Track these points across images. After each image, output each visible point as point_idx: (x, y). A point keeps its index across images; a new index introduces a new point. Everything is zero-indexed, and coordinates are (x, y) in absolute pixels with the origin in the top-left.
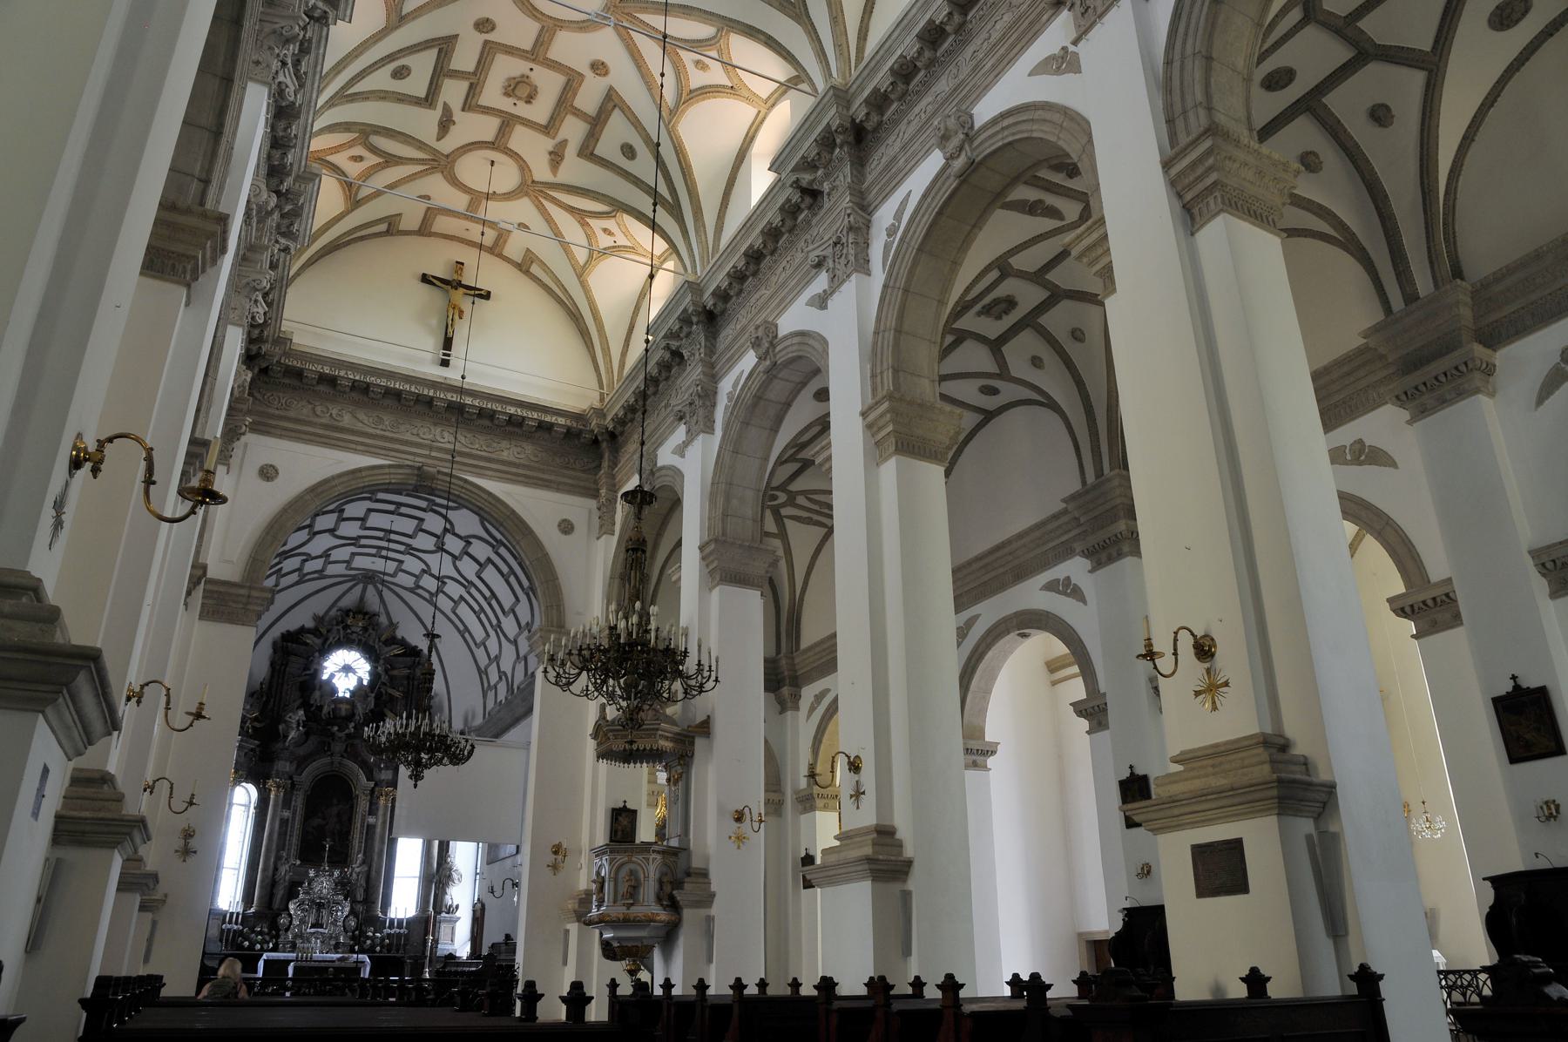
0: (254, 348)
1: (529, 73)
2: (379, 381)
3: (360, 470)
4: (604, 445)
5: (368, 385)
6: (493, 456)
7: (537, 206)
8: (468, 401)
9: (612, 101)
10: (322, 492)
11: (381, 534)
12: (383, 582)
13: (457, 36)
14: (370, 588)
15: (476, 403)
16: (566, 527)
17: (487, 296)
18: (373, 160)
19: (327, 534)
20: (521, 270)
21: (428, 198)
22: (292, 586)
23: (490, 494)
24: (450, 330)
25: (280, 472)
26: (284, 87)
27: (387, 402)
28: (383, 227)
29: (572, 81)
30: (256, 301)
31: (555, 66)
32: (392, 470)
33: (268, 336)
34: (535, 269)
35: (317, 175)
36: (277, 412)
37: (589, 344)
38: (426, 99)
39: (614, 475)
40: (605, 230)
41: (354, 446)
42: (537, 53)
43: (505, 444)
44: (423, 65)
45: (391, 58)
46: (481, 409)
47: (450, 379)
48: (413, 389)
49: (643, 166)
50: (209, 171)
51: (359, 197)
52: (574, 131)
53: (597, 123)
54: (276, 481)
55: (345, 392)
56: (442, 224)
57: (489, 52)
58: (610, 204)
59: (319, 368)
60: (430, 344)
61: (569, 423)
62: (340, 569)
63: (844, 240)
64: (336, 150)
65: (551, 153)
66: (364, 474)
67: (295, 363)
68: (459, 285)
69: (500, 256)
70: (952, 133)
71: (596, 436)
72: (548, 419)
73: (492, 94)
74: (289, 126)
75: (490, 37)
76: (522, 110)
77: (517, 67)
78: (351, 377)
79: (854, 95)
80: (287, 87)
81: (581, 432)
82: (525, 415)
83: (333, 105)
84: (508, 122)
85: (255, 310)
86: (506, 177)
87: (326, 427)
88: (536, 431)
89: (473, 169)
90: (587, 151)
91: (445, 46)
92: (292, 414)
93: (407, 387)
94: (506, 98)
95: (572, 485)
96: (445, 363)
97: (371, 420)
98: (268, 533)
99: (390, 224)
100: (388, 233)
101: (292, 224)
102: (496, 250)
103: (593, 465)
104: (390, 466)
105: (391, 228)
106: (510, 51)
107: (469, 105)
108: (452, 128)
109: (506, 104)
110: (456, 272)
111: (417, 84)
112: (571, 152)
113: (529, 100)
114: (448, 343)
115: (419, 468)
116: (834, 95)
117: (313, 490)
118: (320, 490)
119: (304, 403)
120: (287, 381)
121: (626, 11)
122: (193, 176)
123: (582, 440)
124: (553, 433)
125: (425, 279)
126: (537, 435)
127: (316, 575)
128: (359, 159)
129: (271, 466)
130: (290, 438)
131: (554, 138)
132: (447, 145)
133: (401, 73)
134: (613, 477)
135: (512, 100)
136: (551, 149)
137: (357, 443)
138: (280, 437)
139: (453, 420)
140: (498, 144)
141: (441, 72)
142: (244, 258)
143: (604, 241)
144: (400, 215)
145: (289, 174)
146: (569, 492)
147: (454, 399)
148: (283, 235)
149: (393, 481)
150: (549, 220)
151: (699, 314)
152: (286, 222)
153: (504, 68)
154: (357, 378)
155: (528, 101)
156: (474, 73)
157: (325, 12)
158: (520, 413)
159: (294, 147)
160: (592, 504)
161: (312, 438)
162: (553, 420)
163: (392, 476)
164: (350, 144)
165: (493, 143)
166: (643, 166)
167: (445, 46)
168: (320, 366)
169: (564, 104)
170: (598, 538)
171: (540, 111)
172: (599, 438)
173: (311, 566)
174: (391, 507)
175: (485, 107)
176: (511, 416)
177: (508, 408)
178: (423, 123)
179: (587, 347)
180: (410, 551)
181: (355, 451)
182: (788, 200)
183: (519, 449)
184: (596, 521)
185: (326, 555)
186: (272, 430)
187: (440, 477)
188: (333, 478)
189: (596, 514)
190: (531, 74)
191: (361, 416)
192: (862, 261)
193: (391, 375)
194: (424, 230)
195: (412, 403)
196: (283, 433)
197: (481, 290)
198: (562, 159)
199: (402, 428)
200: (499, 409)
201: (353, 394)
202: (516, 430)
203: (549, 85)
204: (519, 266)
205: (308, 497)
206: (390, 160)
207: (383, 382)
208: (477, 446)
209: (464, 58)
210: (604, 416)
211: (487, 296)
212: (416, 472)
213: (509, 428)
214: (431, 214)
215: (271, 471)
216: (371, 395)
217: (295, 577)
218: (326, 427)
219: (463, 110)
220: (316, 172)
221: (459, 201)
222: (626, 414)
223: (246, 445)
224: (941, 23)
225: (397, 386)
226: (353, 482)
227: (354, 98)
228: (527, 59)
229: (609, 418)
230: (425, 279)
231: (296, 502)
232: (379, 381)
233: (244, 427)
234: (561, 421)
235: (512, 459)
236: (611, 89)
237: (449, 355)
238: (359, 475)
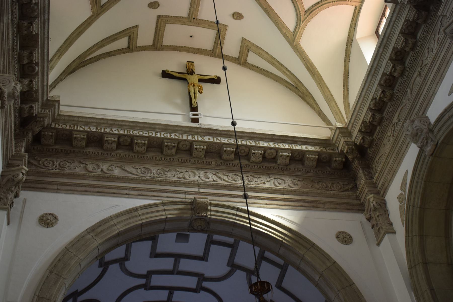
5: (132, 138)
8: (225, 140)
10: (102, 231)
20: (239, 64)
24: (193, 100)
25: (59, 218)
27: (151, 155)
34: (252, 58)
37: (312, 102)
39: (375, 184)
48: (173, 136)
51: (102, 4)
54: (56, 227)
55: (111, 150)
59: (86, 129)
61: (318, 149)
66: (140, 212)
67: (64, 127)
71: (346, 158)
78: (116, 132)
81: (330, 156)
82: (277, 146)
87: (98, 178)
88: (290, 164)
92: (66, 171)
95: (337, 203)
97: (139, 170)
98: (51, 272)
99: (130, 37)
103: (351, 186)
115: (191, 203)
117: (92, 229)
118: (99, 229)
119: (76, 163)
120: (58, 147)
123: (334, 165)
124: (306, 162)
125: (166, 75)
126: (292, 166)
129: (50, 214)
130: (67, 191)
134: (375, 185)
137: (129, 189)
138: (57, 191)
139: (214, 163)
144: (137, 26)
146: (336, 209)
149: (169, 216)
154: (122, 132)
161: (88, 189)
162: (304, 148)
163: (167, 212)
170: (378, 245)
172: (350, 157)
176: (265, 149)
179: (310, 105)
184: (371, 233)
186: (49, 186)
188: (111, 218)
191: (129, 168)
193: (151, 126)
195: (174, 151)
196: (59, 187)
200: (253, 144)
201: (120, 152)
202: (273, 165)
205: (89, 237)
210: (349, 134)
212: (189, 207)
213: (266, 164)
216: (136, 148)
218: (98, 178)
222: (373, 116)
223: (25, 201)
226: (131, 221)
229: (355, 133)
230: (166, 75)
232: (141, 133)
233: (21, 174)
237: (197, 115)
238: (135, 213)
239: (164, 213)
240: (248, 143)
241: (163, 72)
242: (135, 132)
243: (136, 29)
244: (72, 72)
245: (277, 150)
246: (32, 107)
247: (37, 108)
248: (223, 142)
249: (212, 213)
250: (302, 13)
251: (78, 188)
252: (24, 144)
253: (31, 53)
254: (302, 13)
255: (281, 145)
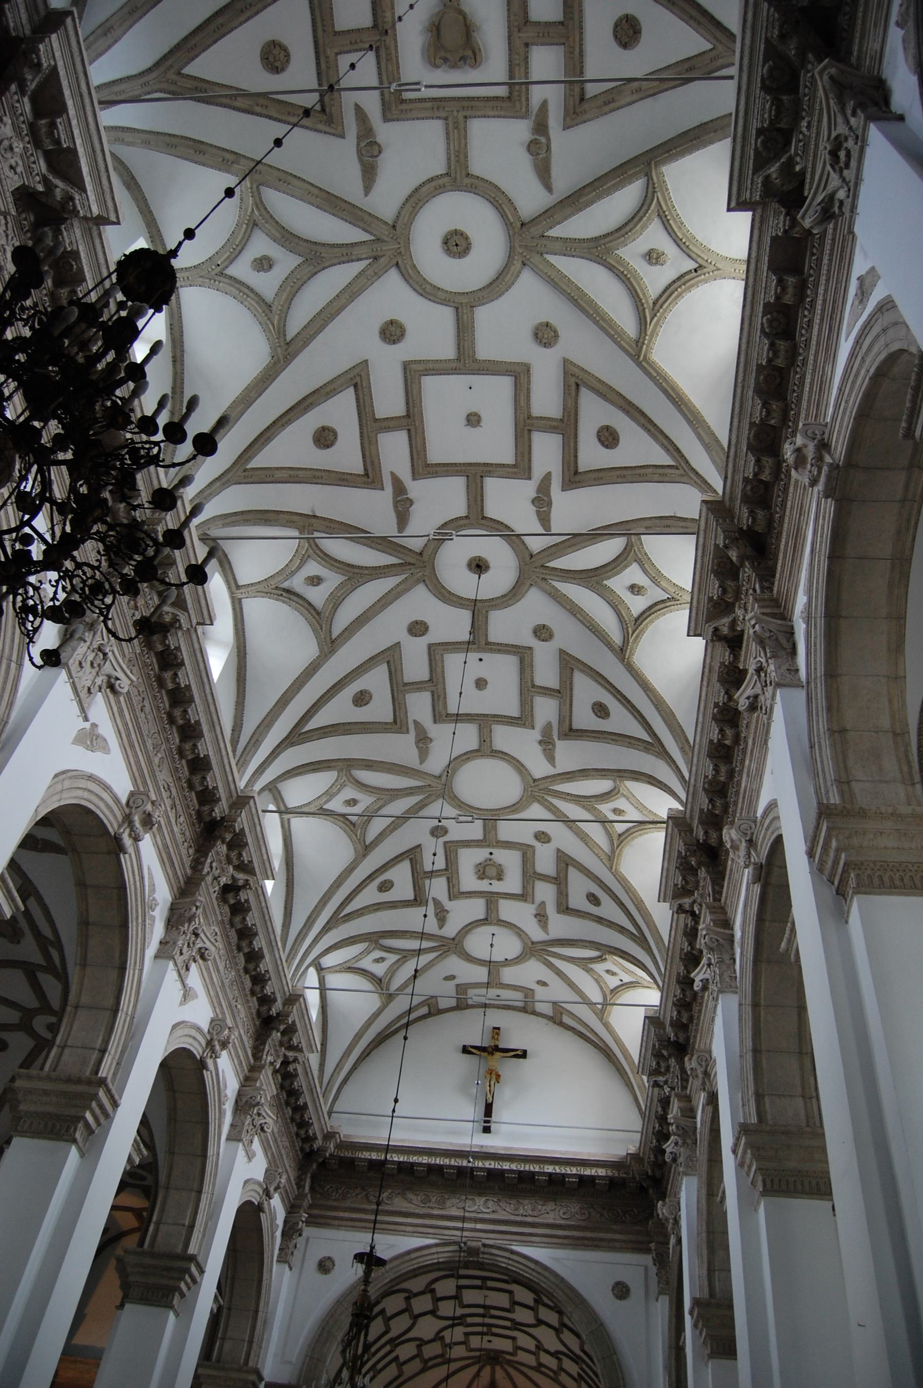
0: (307, 1147)
1: (489, 856)
2: (420, 1159)
3: (409, 1253)
4: (651, 1191)
5: (412, 1164)
6: (537, 1220)
7: (544, 963)
8: (506, 1166)
9: (564, 861)
11: (481, 1311)
12: (509, 1362)
13: (419, 846)
14: (498, 1368)
15: (514, 1167)
16: (621, 1291)
17: (523, 1055)
18: (392, 958)
19: (429, 1316)
21: (452, 977)
22: (418, 1374)
23: (537, 1262)
26: (203, 951)
28: (424, 1010)
29: (527, 853)
30: (259, 1114)
31: (508, 845)
32: (440, 1249)
33: (315, 1134)
34: (566, 1020)
35: (300, 996)
36: (335, 1204)
38: (415, 899)
40: (608, 971)
41: (403, 1228)
42: (489, 840)
43: (550, 1206)
44: (402, 875)
45: (371, 878)
46: (520, 1172)
47: (486, 1146)
48: (453, 1162)
49: (609, 910)
50: (106, 1041)
52: (545, 892)
53: (560, 881)
56: (474, 996)
57: (451, 850)
58: (598, 949)
60: (471, 1111)
61: (610, 1174)
62: (458, 1351)
63: (713, 961)
64: (358, 958)
65: (536, 916)
66: (413, 1256)
68: (497, 1049)
69: (534, 1013)
70: (738, 843)
72: (588, 1172)
73: (468, 880)
74: (257, 966)
75: (446, 838)
76: (497, 887)
77: (481, 854)
78: (396, 1159)
79: (691, 818)
80: (206, 949)
81: (624, 1179)
82: (563, 1171)
83: (330, 929)
84: (492, 899)
85: (263, 1121)
86: (509, 947)
89: (477, 943)
90: (564, 908)
91: (413, 855)
93: (447, 1161)
94: (479, 881)
96: (487, 1130)
99: (429, 1006)
100: (429, 1015)
101: (291, 1039)
102: (527, 1009)
104: (436, 1245)
105: (433, 1010)
106: (467, 844)
107: (455, 893)
108: (448, 916)
109: (483, 886)
110: (493, 1037)
111: (403, 888)
112: (551, 910)
113: (500, 878)
114: (488, 1110)
116: (673, 824)
121: (541, 787)
122: (94, 1049)
125: (466, 1050)
127: (439, 1360)
128: (381, 960)
131: (533, 903)
132: (451, 930)
133: (385, 886)
135: (486, 882)
136: (535, 912)
138: (338, 1227)
140: (490, 918)
141: (419, 877)
142: (247, 1079)
143: (613, 982)
145: (275, 1000)
147: (492, 1166)
148: (291, 1048)
149: (441, 1260)
150: (559, 973)
151: (665, 1047)
152: (286, 1038)
153: (468, 860)
154: (401, 1159)
155: (500, 878)
156: (446, 870)
157: (247, 880)
158: (558, 1171)
159: (270, 979)
160: (647, 1259)
163: (440, 1255)
164: (367, 952)
165: (486, 919)
166: (609, 910)
167: (413, 855)
168: (368, 1153)
169: (530, 875)
171: (512, 883)
173: (430, 1351)
174: (478, 1282)
175: (467, 893)
176: (550, 1174)
177: (546, 1167)
178: (412, 918)
180: (395, 1342)
181: (405, 1233)
182: (686, 925)
183: (565, 1210)
185: (438, 1337)
187: (486, 1250)
189: (653, 1270)
190: (492, 857)
192: (728, 979)
194: (461, 1005)
196: (341, 1223)
197: (516, 1050)
198: (547, 919)
199: (449, 1203)
200: (537, 1170)
203: (510, 860)
204: (551, 1019)
206: (406, 955)
207: (425, 1160)
208: (521, 1212)
209: (434, 859)
211: (523, 1055)
214: (462, 989)
215: (328, 1263)
217: (417, 1365)
219: (450, 900)
220: (300, 993)
221: (480, 974)
224: (719, 740)
225: (438, 1162)
227: (350, 917)
228: (482, 847)
230: (466, 1050)
231: (351, 1292)
232: (420, 1159)
234: (601, 1172)
235: (551, 1221)
236: (558, 851)
239: (436, 1256)
240: (532, 1168)
241: (464, 1047)
242: (415, 1158)
243: (434, 999)
244: (367, 1055)
245: (564, 1176)
246: (312, 1146)
247: (319, 1143)
248: (505, 1167)
249: (486, 1256)
250: (608, 993)
251: (357, 1224)
252: (309, 1175)
253: (302, 1116)
254: (608, 993)
255: (568, 1169)
